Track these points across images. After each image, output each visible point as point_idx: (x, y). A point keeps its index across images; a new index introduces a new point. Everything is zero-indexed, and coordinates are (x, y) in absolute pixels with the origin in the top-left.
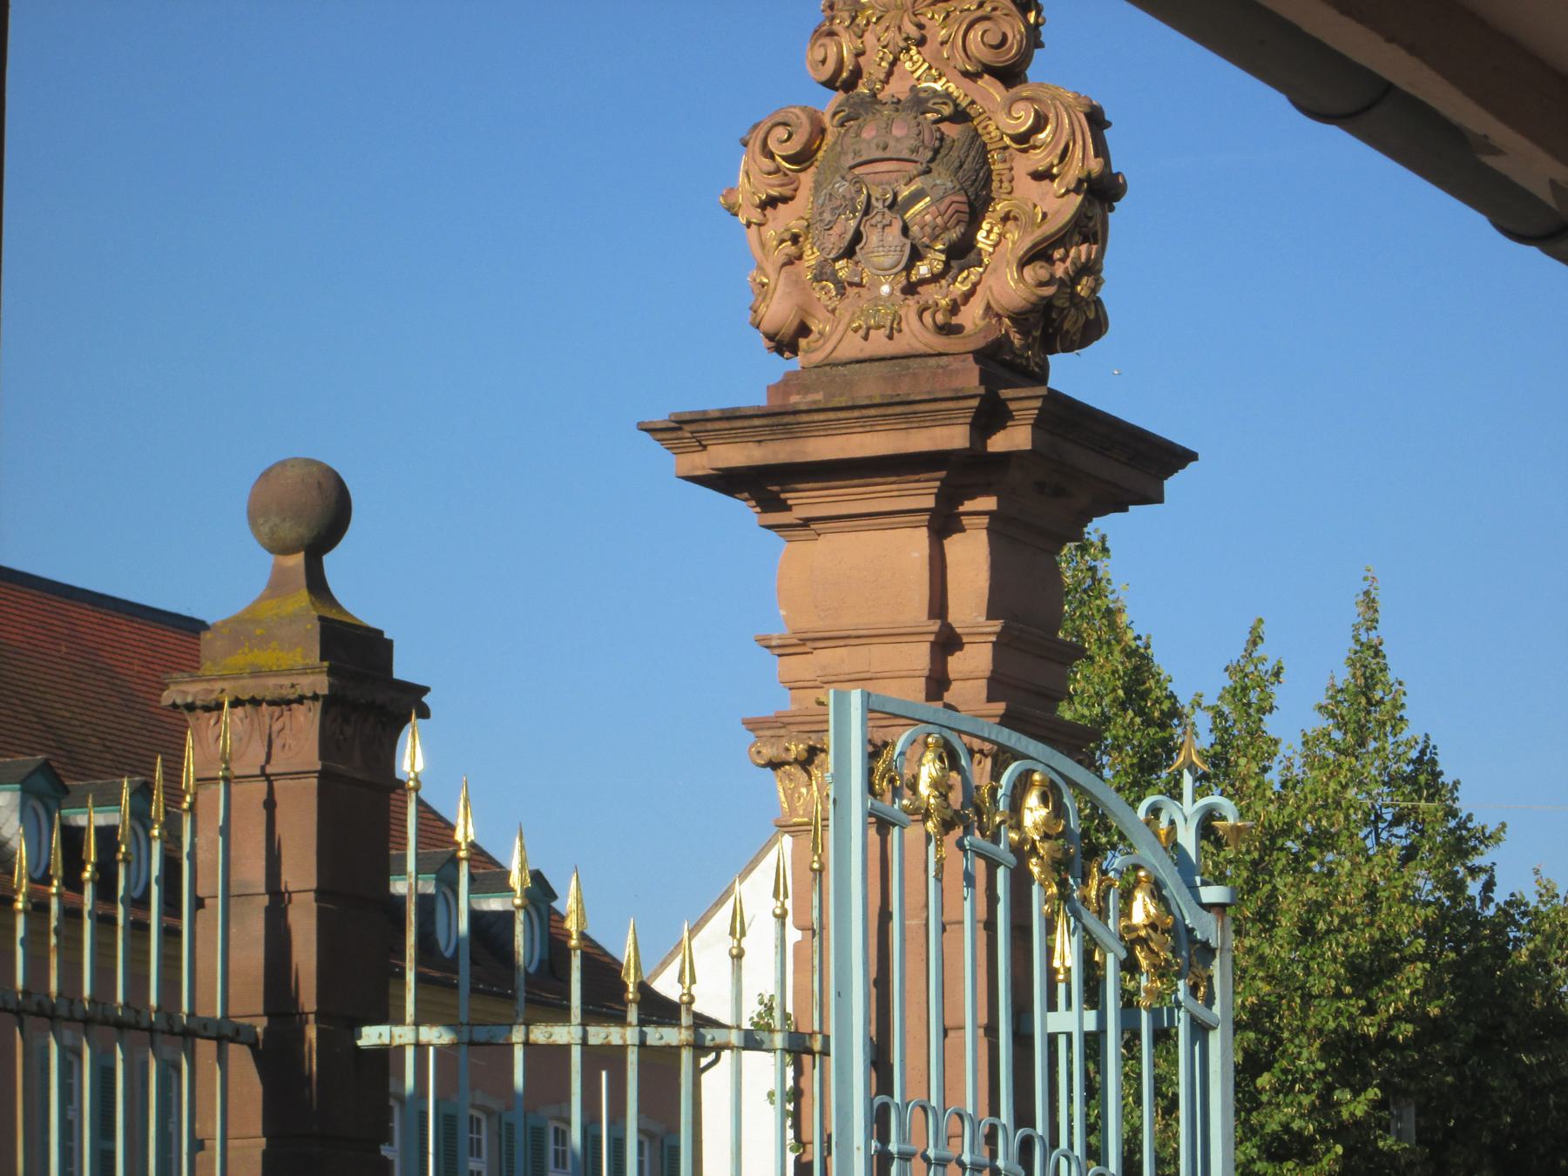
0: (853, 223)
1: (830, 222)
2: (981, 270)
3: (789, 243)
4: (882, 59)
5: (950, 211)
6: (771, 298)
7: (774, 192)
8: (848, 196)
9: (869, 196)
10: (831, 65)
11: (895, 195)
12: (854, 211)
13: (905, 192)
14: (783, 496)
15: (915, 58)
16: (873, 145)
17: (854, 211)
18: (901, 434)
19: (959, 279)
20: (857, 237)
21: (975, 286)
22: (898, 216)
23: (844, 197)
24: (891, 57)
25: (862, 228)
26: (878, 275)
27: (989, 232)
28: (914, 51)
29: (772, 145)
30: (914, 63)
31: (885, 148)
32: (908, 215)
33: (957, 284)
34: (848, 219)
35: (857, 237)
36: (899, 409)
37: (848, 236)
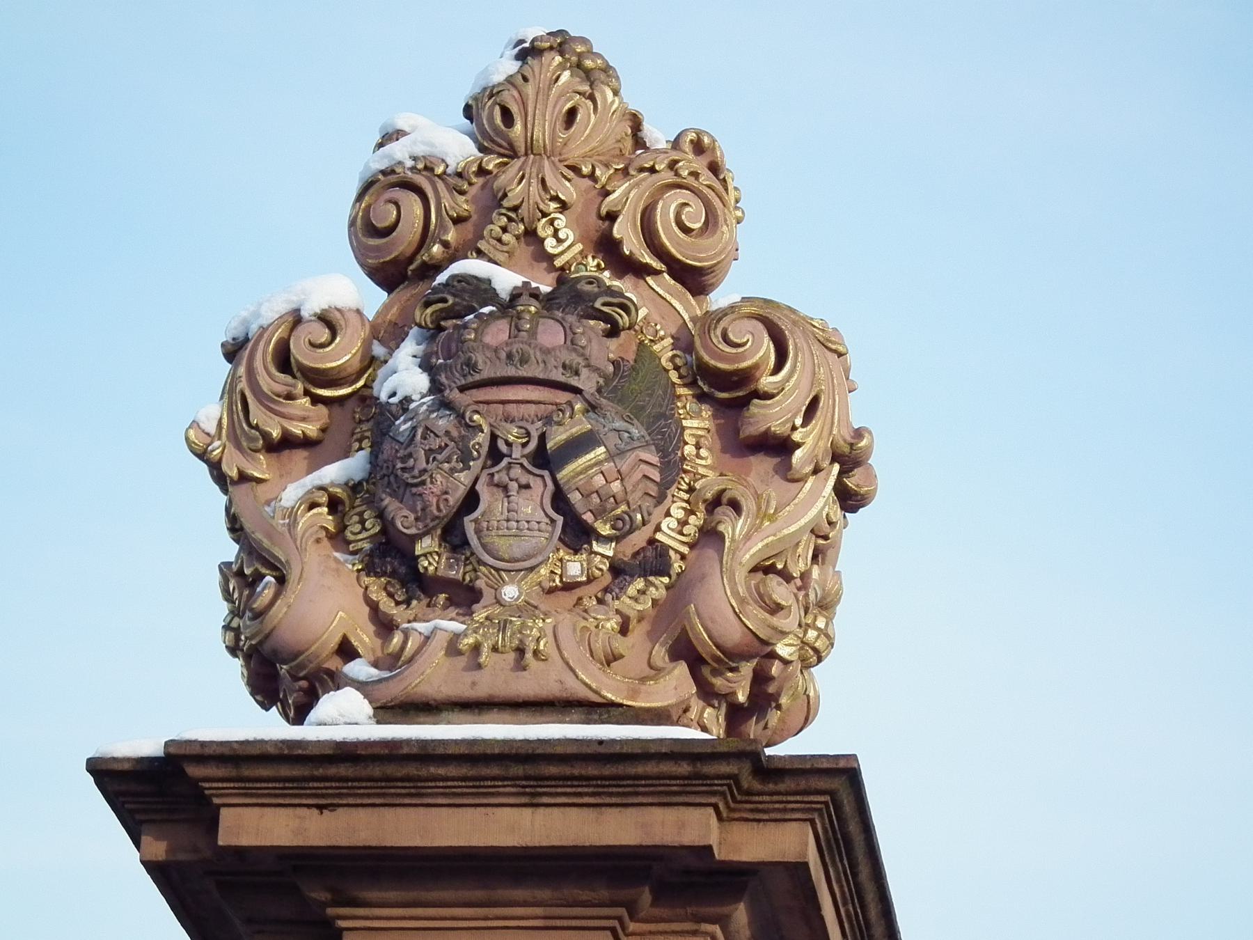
0: (465, 478)
2: (666, 580)
3: (325, 510)
4: (504, 230)
5: (637, 475)
8: (455, 433)
9: (494, 438)
11: (543, 438)
12: (465, 458)
13: (557, 438)
14: (331, 911)
15: (561, 235)
16: (503, 355)
17: (465, 458)
19: (632, 590)
20: (471, 500)
22: (546, 473)
23: (447, 433)
25: (477, 487)
26: (497, 570)
28: (561, 221)
30: (560, 241)
31: (524, 360)
33: (624, 599)
34: (453, 470)
35: (471, 500)
36: (592, 770)
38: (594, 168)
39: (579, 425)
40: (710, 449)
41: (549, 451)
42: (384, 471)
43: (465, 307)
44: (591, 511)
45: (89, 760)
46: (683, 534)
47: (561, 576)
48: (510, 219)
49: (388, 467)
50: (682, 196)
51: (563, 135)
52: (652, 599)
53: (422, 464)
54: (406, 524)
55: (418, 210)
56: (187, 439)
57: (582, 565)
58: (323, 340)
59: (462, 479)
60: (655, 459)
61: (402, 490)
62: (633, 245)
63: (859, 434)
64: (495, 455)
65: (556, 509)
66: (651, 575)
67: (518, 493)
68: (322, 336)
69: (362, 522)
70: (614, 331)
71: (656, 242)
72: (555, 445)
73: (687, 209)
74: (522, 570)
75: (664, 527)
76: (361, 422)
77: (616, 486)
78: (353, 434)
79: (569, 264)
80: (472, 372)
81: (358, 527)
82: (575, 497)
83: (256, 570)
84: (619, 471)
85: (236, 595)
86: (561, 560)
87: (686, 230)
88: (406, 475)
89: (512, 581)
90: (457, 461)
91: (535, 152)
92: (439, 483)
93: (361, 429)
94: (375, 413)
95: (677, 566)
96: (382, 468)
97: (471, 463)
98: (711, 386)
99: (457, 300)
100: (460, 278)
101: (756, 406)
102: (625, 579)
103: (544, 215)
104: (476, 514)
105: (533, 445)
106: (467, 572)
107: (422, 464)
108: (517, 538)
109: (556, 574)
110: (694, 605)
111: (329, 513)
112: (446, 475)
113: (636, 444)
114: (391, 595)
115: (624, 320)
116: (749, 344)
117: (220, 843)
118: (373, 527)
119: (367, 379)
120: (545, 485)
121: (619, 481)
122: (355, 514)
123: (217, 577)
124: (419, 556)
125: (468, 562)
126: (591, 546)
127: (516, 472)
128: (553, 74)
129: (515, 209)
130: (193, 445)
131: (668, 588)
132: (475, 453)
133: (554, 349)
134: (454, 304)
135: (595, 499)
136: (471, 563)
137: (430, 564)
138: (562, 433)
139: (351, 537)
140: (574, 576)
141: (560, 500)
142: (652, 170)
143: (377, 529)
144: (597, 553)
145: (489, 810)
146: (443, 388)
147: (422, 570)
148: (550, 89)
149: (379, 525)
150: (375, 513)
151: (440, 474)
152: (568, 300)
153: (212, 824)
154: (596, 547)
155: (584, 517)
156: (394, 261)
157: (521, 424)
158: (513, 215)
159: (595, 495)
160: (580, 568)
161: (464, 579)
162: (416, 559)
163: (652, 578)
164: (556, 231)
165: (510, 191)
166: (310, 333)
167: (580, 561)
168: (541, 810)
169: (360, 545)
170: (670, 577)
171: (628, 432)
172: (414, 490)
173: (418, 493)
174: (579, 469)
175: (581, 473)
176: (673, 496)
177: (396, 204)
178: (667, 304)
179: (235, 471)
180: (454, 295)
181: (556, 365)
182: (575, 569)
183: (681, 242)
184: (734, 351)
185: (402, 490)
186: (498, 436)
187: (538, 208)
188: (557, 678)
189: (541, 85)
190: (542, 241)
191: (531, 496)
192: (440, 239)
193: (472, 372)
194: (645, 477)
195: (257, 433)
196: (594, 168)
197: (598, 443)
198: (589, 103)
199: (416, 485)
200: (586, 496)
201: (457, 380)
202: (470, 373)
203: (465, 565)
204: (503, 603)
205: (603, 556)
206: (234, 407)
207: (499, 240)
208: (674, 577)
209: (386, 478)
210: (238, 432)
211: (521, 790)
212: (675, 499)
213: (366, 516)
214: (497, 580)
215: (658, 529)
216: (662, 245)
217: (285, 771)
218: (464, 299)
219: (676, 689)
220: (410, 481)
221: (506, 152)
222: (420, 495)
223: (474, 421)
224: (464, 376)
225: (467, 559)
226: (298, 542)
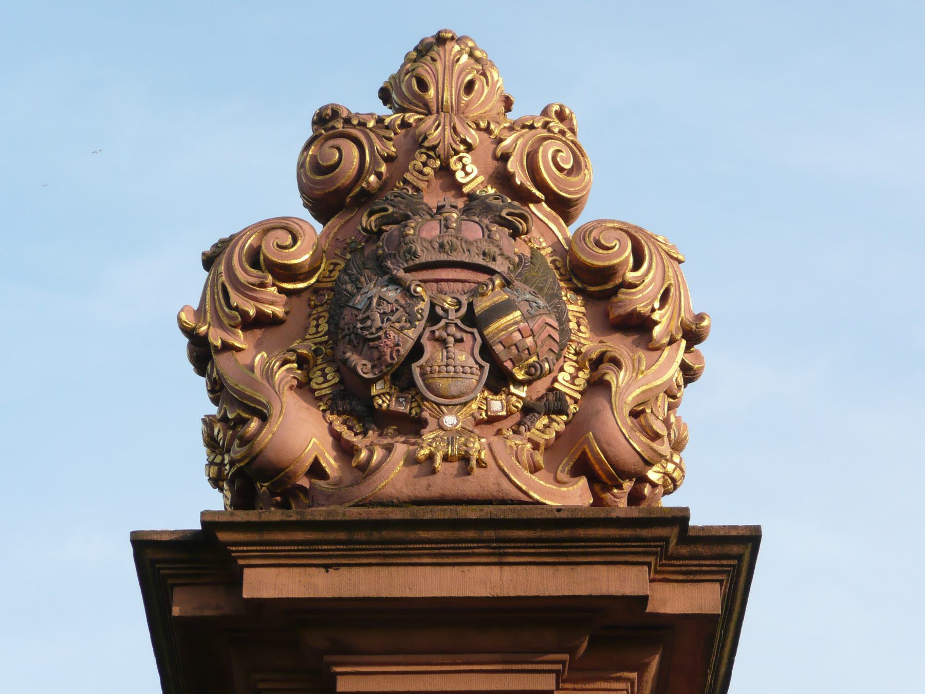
0: (412, 334)
2: (564, 418)
4: (425, 164)
5: (545, 334)
8: (402, 302)
9: (433, 306)
11: (471, 305)
13: (482, 305)
14: (327, 659)
15: (468, 169)
16: (436, 245)
17: (411, 321)
18: (549, 570)
20: (417, 351)
22: (475, 331)
23: (396, 301)
24: (438, 163)
25: (424, 341)
26: (438, 405)
27: (574, 377)
28: (468, 159)
30: (467, 174)
31: (453, 248)
33: (533, 430)
34: (402, 329)
35: (417, 351)
37: (404, 350)
38: (489, 124)
39: (498, 296)
41: (477, 315)
42: (346, 332)
43: (401, 215)
44: (511, 360)
45: (133, 534)
46: (574, 385)
47: (486, 411)
48: (429, 157)
49: (349, 329)
51: (466, 99)
52: (556, 431)
53: (378, 323)
54: (365, 370)
55: (356, 153)
56: (179, 319)
57: (502, 403)
58: (288, 243)
59: (411, 334)
60: (556, 324)
61: (361, 345)
62: (521, 178)
63: (700, 317)
64: (434, 318)
66: (553, 414)
67: (454, 345)
68: (287, 241)
69: (324, 375)
70: (516, 233)
71: (538, 178)
72: (481, 310)
73: (560, 154)
74: (457, 405)
75: (560, 378)
76: (316, 306)
77: (529, 341)
78: (310, 316)
80: (413, 258)
81: (321, 379)
82: (498, 348)
83: (238, 414)
84: (531, 330)
86: (486, 399)
87: (561, 169)
89: (450, 413)
90: (406, 321)
91: (444, 110)
92: (392, 337)
93: (317, 311)
94: (328, 299)
95: (573, 408)
96: (343, 330)
97: (417, 323)
98: (583, 282)
99: (395, 209)
100: (396, 194)
101: (623, 295)
102: (535, 416)
103: (457, 152)
104: (422, 361)
105: (464, 310)
106: (413, 408)
107: (378, 323)
108: (454, 379)
109: (482, 409)
110: (592, 433)
111: (299, 368)
112: (398, 332)
113: (542, 311)
114: (350, 428)
115: (523, 226)
116: (617, 247)
117: (245, 596)
118: (333, 378)
119: (319, 276)
120: (475, 339)
121: (531, 337)
122: (318, 370)
123: (200, 427)
124: (374, 396)
125: (414, 400)
126: (509, 389)
127: (452, 329)
128: (454, 57)
129: (434, 148)
130: (184, 324)
131: (566, 423)
132: (419, 316)
133: (476, 241)
134: (393, 213)
135: (514, 350)
136: (416, 401)
137: (383, 402)
138: (486, 302)
139: (315, 386)
140: (497, 412)
141: (486, 351)
142: (532, 127)
143: (337, 380)
144: (513, 394)
145: (466, 568)
146: (389, 271)
147: (377, 407)
148: (453, 66)
149: (338, 377)
150: (334, 368)
151: (393, 331)
152: (480, 210)
153: (237, 582)
155: (505, 364)
156: (337, 191)
157: (454, 295)
158: (432, 154)
159: (514, 347)
160: (501, 406)
161: (410, 413)
163: (554, 416)
164: (464, 166)
165: (429, 135)
166: (277, 238)
167: (501, 400)
168: (507, 569)
169: (323, 392)
170: (567, 415)
171: (536, 303)
172: (371, 344)
173: (375, 346)
174: (501, 327)
175: (502, 330)
176: (565, 357)
178: (545, 226)
179: (220, 341)
180: (393, 206)
181: (478, 252)
182: (497, 405)
183: (558, 179)
184: (605, 252)
185: (361, 345)
186: (436, 304)
187: (452, 147)
188: (495, 482)
189: (447, 64)
191: (464, 348)
192: (375, 171)
193: (413, 258)
194: (550, 336)
195: (237, 313)
196: (489, 124)
197: (516, 308)
198: (483, 78)
201: (401, 265)
202: (411, 258)
203: (412, 402)
204: (445, 428)
205: (518, 397)
206: (216, 297)
207: (421, 172)
208: (571, 416)
209: (347, 337)
210: (221, 314)
211: (492, 551)
212: (566, 359)
213: (327, 371)
214: (438, 412)
215: (555, 380)
216: (543, 180)
217: (299, 536)
218: (401, 209)
219: (581, 496)
220: (369, 336)
221: (422, 111)
222: (377, 347)
223: (417, 293)
224: (407, 261)
225: (413, 397)
226: (277, 388)
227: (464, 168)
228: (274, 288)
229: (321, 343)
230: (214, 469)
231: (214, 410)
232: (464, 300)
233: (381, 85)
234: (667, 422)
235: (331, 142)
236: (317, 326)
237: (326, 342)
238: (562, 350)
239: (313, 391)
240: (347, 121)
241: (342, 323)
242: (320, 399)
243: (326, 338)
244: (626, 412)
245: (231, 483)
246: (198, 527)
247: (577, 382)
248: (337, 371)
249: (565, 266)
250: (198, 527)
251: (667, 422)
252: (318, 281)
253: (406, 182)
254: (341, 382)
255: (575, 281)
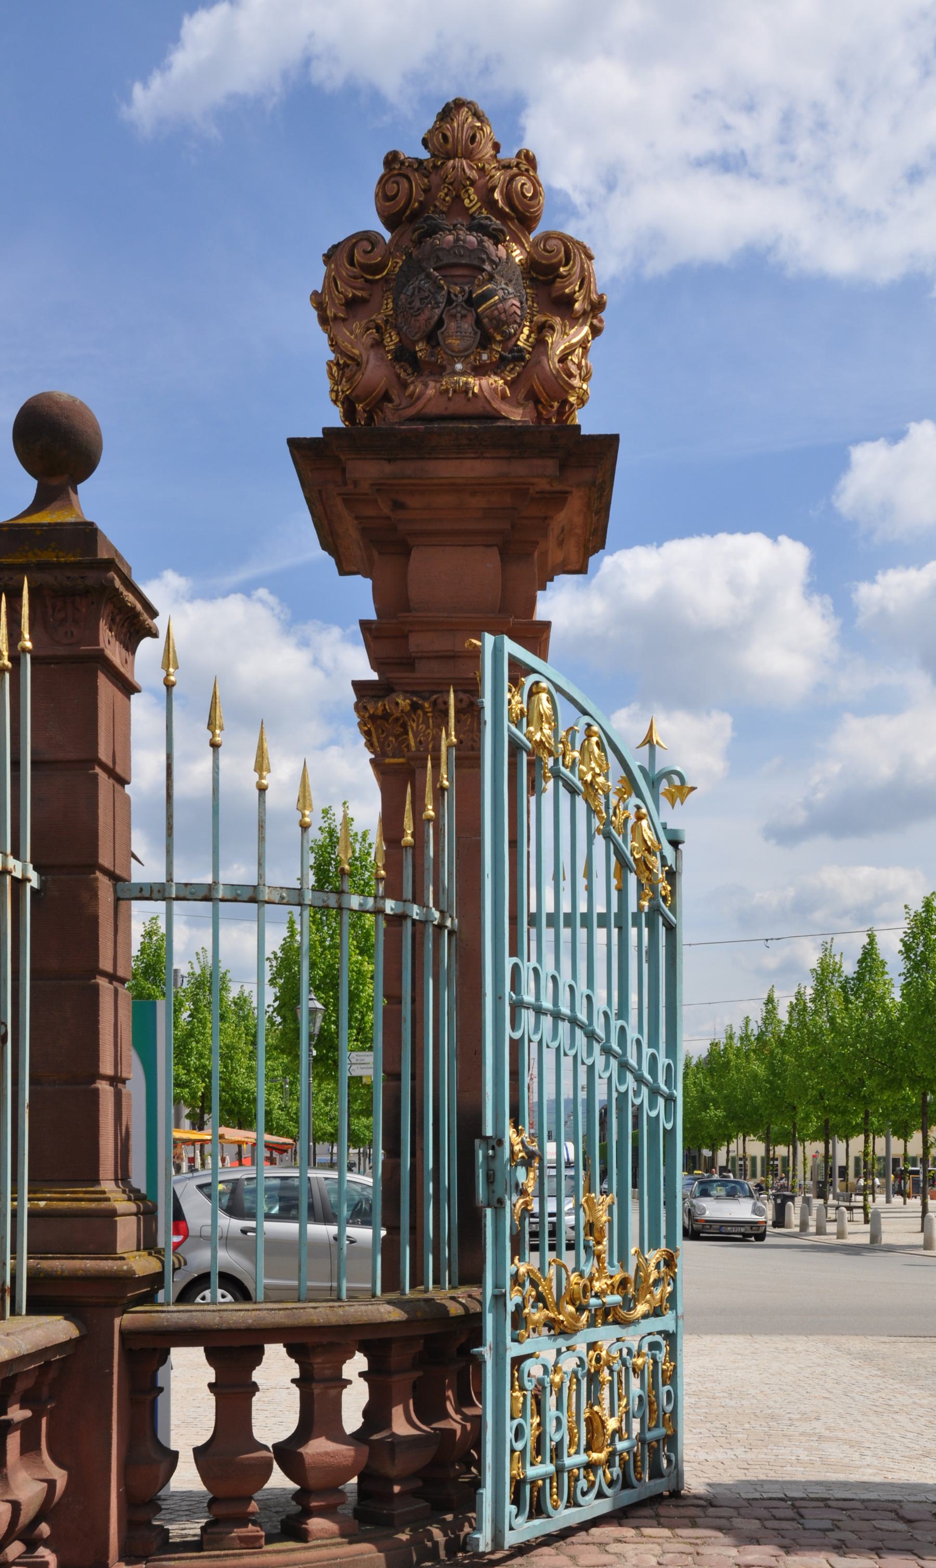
0: (437, 311)
1: (419, 309)
2: (523, 364)
3: (374, 330)
4: (446, 195)
6: (365, 368)
7: (359, 293)
8: (433, 291)
9: (449, 293)
10: (401, 201)
11: (471, 293)
15: (472, 197)
19: (508, 369)
21: (519, 375)
22: (473, 309)
23: (429, 290)
25: (444, 316)
26: (452, 357)
27: (529, 336)
29: (357, 257)
30: (471, 201)
32: (479, 310)
34: (433, 308)
35: (440, 323)
40: (538, 304)
46: (528, 342)
50: (523, 179)
51: (471, 146)
55: (407, 185)
60: (518, 304)
64: (450, 301)
65: (478, 327)
73: (526, 186)
75: (521, 338)
76: (386, 291)
78: (383, 297)
79: (475, 212)
82: (486, 321)
85: (336, 374)
86: (479, 353)
88: (412, 311)
89: (459, 362)
98: (537, 273)
101: (558, 283)
103: (465, 187)
105: (466, 296)
113: (511, 296)
114: (405, 371)
123: (326, 367)
127: (459, 309)
129: (451, 184)
131: (524, 367)
139: (387, 344)
141: (478, 322)
143: (398, 340)
144: (494, 350)
148: (464, 124)
154: (494, 347)
158: (450, 187)
162: (416, 352)
163: (516, 363)
177: (398, 184)
180: (428, 225)
190: (463, 201)
199: (416, 316)
200: (491, 320)
207: (444, 200)
210: (334, 296)
227: (469, 198)
228: (362, 279)
229: (389, 316)
230: (334, 395)
231: (332, 356)
232: (467, 288)
233: (422, 136)
234: (579, 366)
235: (393, 179)
236: (387, 304)
237: (392, 315)
238: (522, 320)
239: (385, 347)
240: (402, 163)
241: (400, 303)
242: (388, 352)
243: (392, 312)
244: (556, 360)
245: (343, 403)
246: (321, 435)
247: (531, 340)
248: (398, 334)
249: (526, 262)
250: (321, 435)
251: (579, 366)
252: (387, 274)
253: (435, 206)
254: (400, 341)
255: (532, 273)
